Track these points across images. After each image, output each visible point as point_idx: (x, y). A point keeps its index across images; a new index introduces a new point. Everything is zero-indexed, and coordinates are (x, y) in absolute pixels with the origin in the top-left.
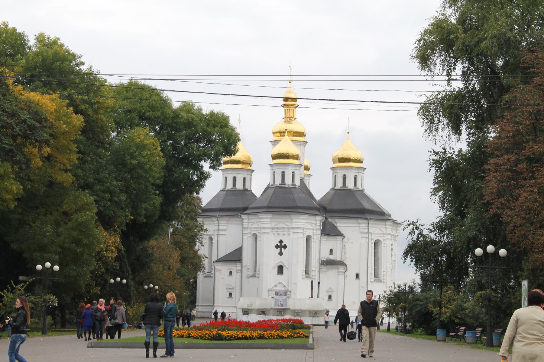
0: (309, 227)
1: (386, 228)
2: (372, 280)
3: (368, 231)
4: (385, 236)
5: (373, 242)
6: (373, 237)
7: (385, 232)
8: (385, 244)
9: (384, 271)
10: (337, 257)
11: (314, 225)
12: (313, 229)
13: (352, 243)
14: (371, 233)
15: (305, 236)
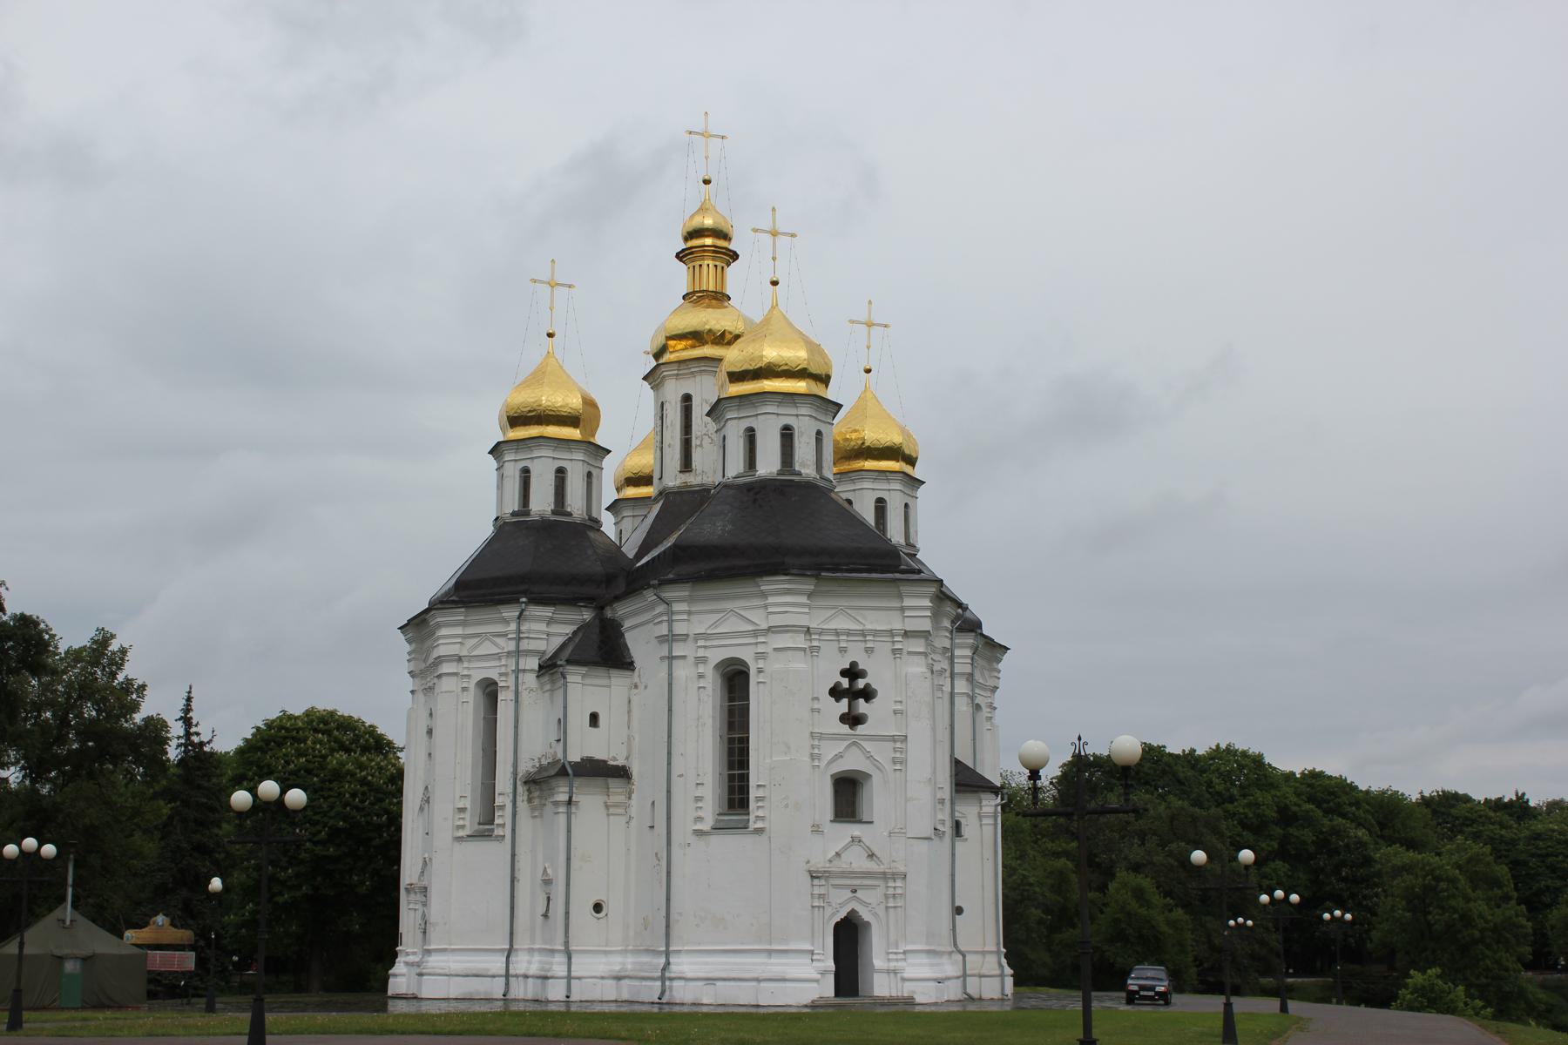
0: (487, 648)
1: (766, 607)
2: (699, 826)
3: (670, 630)
4: (761, 639)
5: (708, 670)
6: (701, 653)
7: (764, 626)
8: (760, 671)
9: (759, 786)
10: (584, 745)
11: (500, 641)
12: (498, 657)
13: (646, 687)
14: (698, 637)
15: (472, 685)
